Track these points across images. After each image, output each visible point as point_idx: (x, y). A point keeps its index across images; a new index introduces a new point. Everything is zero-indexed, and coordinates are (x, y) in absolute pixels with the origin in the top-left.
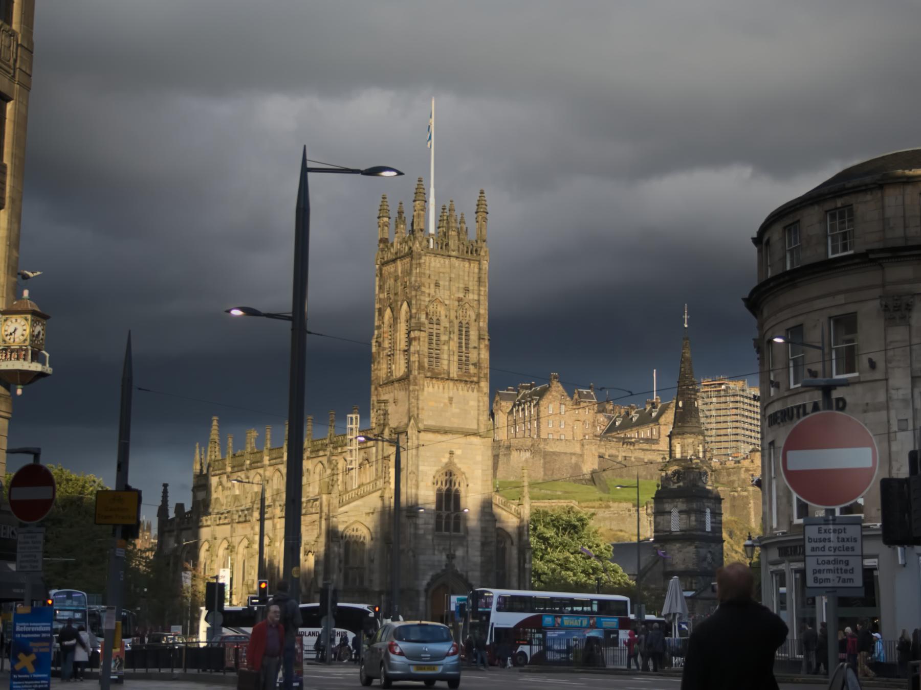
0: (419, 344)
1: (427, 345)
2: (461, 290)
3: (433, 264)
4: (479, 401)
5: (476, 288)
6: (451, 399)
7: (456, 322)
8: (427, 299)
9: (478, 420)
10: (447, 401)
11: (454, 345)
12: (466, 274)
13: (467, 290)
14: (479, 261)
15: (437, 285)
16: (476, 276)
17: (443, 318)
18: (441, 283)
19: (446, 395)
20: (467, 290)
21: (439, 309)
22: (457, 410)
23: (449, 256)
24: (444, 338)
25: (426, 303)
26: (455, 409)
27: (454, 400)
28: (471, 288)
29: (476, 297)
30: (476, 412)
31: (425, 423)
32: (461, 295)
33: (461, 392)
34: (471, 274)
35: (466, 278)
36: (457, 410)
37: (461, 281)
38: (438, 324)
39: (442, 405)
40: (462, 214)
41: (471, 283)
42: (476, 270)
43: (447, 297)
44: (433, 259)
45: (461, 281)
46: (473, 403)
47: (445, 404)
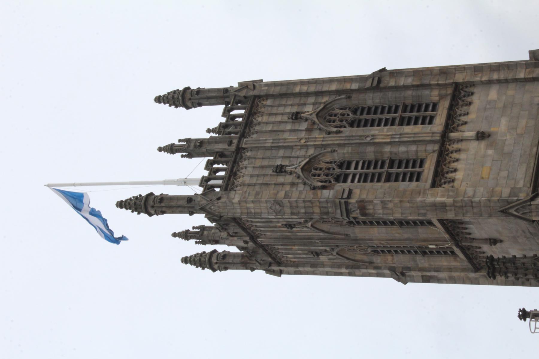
0: (371, 202)
1: (377, 185)
2: (297, 127)
3: (247, 180)
4: (490, 82)
5: (297, 100)
6: (481, 136)
7: (347, 131)
8: (301, 187)
9: (526, 80)
10: (483, 144)
11: (382, 133)
12: (273, 119)
13: (296, 117)
14: (255, 97)
15: (280, 170)
16: (277, 102)
17: (337, 157)
18: (279, 162)
19: (474, 145)
20: (296, 117)
21: (323, 165)
22: (504, 122)
23: (239, 150)
24: (370, 153)
25: (308, 188)
26: (501, 127)
27: (484, 128)
28: (295, 109)
29: (312, 100)
30: (512, 86)
31: (521, 184)
32: (304, 126)
33: (472, 116)
34: (274, 111)
35: (279, 118)
36: (504, 122)
37: (282, 127)
38: (349, 164)
39: (490, 152)
40: (209, 131)
41: (288, 110)
42: (269, 102)
43: (302, 153)
44: (240, 180)
45: (282, 127)
46: (493, 93)
47: (490, 146)
